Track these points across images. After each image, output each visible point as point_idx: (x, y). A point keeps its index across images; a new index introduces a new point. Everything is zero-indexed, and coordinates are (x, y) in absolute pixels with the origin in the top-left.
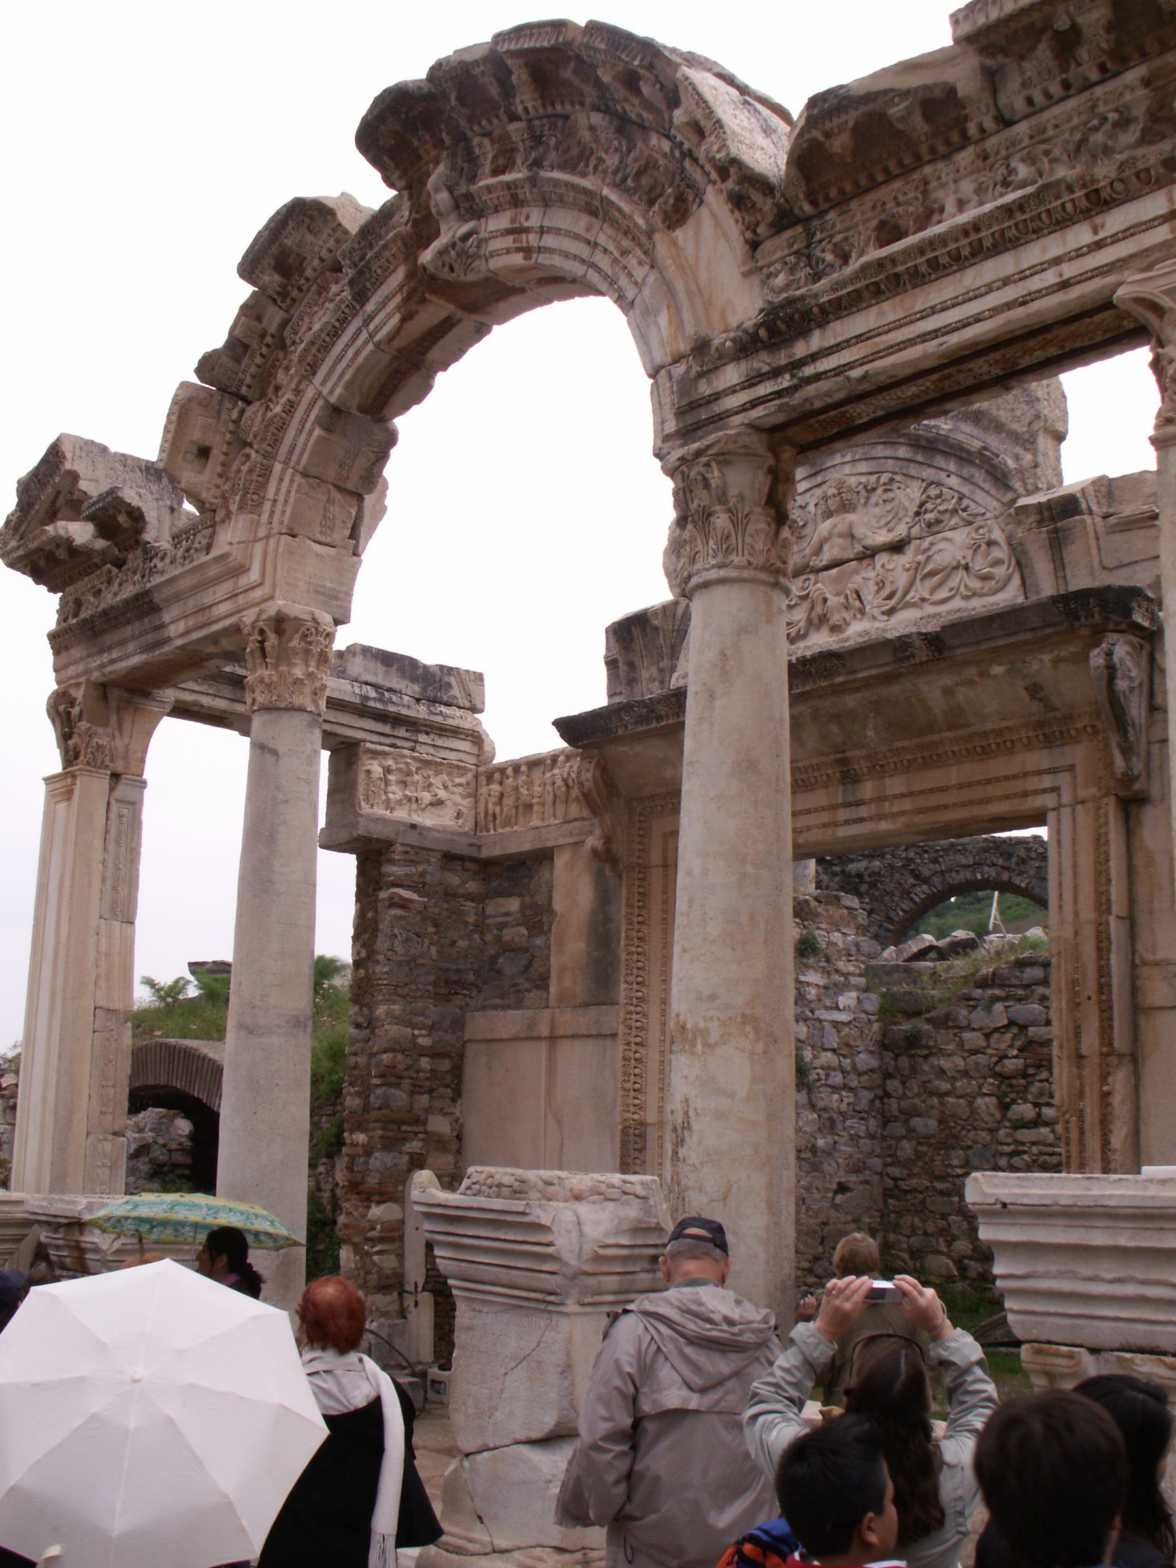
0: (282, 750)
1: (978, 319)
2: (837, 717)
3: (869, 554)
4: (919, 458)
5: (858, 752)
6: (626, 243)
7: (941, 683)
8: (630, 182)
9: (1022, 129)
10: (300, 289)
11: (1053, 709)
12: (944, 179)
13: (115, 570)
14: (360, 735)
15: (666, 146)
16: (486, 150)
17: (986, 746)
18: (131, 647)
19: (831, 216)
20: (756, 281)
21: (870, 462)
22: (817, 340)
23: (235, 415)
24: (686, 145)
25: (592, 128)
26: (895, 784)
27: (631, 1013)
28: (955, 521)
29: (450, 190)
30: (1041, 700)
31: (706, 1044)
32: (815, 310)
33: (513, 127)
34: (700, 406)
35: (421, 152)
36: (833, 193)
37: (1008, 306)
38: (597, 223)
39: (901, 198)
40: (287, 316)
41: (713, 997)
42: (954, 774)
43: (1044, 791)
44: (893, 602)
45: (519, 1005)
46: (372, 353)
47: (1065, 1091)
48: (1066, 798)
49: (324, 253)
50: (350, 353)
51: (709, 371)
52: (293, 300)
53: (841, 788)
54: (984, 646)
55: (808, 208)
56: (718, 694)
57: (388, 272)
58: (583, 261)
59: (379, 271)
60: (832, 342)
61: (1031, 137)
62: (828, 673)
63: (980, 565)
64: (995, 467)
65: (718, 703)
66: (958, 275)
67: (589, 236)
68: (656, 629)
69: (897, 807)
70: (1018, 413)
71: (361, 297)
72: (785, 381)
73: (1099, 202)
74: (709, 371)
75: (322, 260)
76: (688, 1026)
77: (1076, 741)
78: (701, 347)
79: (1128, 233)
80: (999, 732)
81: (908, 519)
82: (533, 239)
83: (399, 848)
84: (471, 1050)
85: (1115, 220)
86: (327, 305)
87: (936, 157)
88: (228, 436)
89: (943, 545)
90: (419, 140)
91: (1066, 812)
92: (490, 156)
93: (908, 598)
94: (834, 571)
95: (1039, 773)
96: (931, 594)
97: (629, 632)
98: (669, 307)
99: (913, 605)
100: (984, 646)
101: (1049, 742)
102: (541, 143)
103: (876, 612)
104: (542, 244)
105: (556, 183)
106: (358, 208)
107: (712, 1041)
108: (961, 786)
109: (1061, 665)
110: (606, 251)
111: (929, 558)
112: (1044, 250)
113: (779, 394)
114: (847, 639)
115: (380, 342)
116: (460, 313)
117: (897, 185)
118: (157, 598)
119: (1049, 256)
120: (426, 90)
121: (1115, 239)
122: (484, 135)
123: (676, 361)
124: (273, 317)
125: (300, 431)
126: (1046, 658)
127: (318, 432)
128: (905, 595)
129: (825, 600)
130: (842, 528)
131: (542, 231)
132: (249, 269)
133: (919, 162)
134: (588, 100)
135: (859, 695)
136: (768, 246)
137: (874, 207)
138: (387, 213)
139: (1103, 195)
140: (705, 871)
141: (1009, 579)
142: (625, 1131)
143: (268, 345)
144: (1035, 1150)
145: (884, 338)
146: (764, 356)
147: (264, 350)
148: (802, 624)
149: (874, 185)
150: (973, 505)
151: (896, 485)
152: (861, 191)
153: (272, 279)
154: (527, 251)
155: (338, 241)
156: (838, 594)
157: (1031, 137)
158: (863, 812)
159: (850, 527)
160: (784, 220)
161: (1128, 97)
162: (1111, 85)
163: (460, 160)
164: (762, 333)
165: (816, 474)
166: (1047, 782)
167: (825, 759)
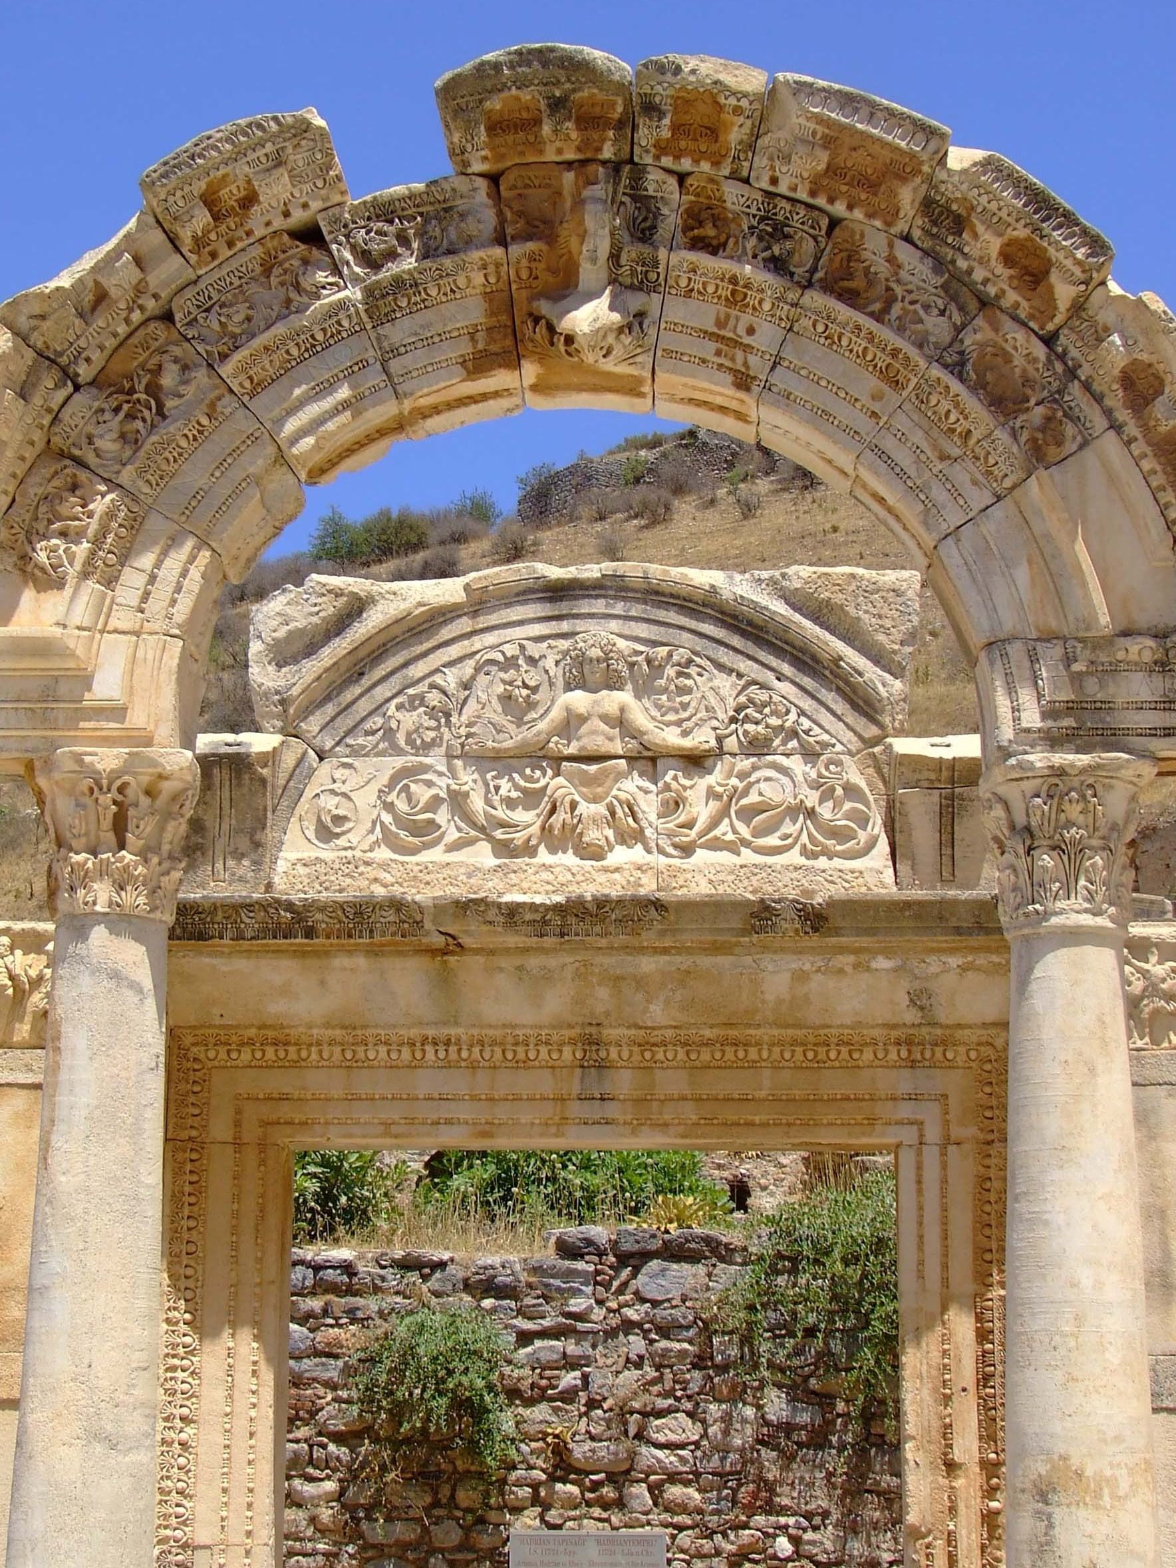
7: (794, 966)
10: (230, 244)
15: (1040, 351)
21: (654, 628)
25: (891, 259)
27: (173, 1369)
30: (922, 1008)
31: (1113, 1496)
38: (893, 398)
43: (900, 1123)
44: (693, 834)
48: (933, 1134)
52: (213, 255)
53: (578, 1071)
64: (854, 688)
65: (1102, 1080)
67: (876, 407)
77: (951, 1066)
81: (715, 723)
90: (556, 131)
91: (931, 1156)
93: (717, 832)
94: (593, 768)
95: (894, 1099)
98: (1030, 562)
101: (913, 1064)
102: (787, 237)
103: (664, 842)
104: (772, 380)
107: (1121, 1493)
109: (969, 973)
114: (617, 870)
123: (1048, 638)
124: (169, 270)
126: (954, 961)
129: (574, 805)
135: (667, 958)
143: (141, 308)
148: (535, 829)
150: (817, 730)
151: (693, 670)
154: (743, 382)
156: (595, 800)
158: (612, 1110)
159: (622, 710)
166: (905, 1111)
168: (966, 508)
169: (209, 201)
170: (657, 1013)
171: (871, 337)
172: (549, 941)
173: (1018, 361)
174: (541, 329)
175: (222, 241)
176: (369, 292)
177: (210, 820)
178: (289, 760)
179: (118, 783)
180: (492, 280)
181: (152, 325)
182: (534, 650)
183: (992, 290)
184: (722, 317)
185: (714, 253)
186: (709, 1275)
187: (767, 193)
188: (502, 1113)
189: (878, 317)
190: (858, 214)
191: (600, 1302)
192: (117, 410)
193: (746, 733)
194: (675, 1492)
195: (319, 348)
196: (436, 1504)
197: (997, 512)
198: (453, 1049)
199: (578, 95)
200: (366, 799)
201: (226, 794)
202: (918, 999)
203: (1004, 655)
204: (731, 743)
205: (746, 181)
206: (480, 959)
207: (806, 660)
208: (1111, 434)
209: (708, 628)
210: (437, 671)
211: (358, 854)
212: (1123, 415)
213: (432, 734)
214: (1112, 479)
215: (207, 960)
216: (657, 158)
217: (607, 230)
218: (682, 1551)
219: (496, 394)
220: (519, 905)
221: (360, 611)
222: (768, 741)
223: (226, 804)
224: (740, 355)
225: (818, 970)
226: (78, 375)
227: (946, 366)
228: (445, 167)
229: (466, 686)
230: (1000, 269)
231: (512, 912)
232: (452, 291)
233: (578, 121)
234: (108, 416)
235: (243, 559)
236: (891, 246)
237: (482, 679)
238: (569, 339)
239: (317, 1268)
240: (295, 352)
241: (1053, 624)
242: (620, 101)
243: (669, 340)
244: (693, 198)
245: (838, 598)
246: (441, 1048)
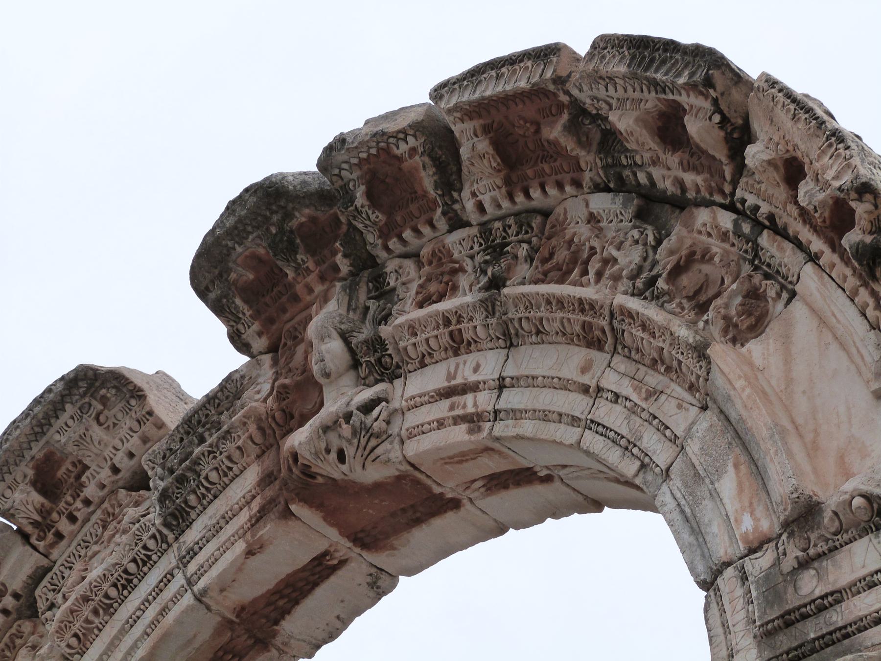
6: (654, 379)
8: (661, 284)
10: (72, 519)
15: (726, 220)
16: (405, 277)
24: (765, 208)
25: (593, 219)
29: (345, 337)
34: (805, 617)
35: (299, 288)
38: (600, 358)
40: (45, 562)
46: (189, 610)
49: (120, 460)
50: (151, 613)
51: (820, 556)
52: (59, 536)
57: (228, 475)
58: (575, 421)
59: (213, 476)
67: (586, 379)
71: (178, 519)
74: (820, 556)
75: (115, 470)
78: (804, 515)
82: (484, 400)
86: (117, 538)
90: (297, 269)
92: (414, 287)
98: (736, 466)
102: (502, 254)
104: (502, 405)
105: (529, 303)
106: (181, 396)
115: (205, 592)
116: (344, 546)
120: (315, 186)
122: (405, 256)
131: (501, 386)
134: (587, 177)
138: (230, 390)
155: (145, 440)
163: (362, 295)
173: (717, 247)
175: (64, 518)
180: (258, 439)
184: (452, 370)
195: (135, 581)
199: (294, 224)
208: (809, 268)
217: (335, 334)
224: (469, 398)
228: (238, 360)
232: (230, 469)
233: (312, 251)
240: (113, 593)
243: (413, 419)
244: (427, 268)
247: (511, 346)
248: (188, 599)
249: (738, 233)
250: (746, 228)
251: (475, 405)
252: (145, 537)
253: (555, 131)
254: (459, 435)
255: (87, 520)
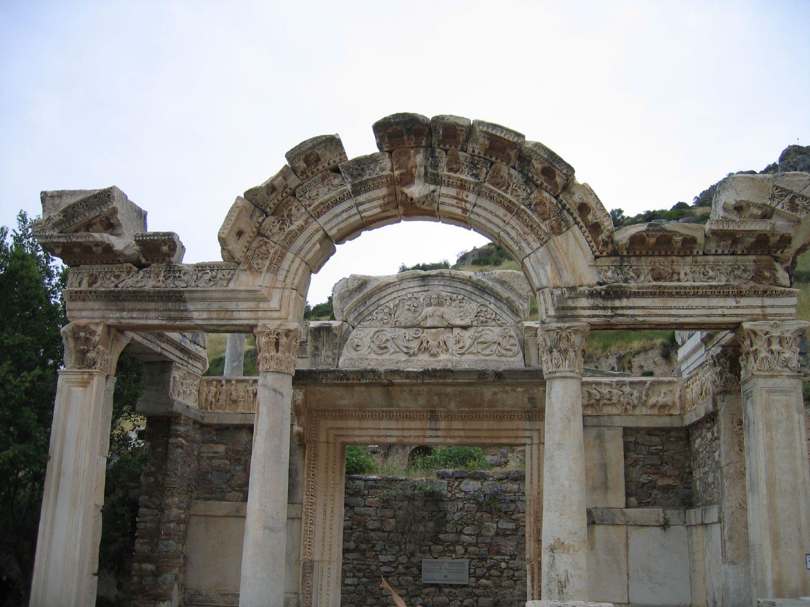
0: (285, 393)
1: (691, 316)
2: (439, 395)
3: (451, 327)
4: (477, 293)
5: (442, 409)
6: (527, 230)
7: (493, 390)
9: (711, 258)
11: (536, 407)
12: (680, 263)
13: (135, 269)
14: (174, 358)
15: (554, 201)
17: (501, 416)
18: (152, 314)
19: (633, 259)
20: (595, 269)
22: (625, 302)
23: (260, 220)
25: (509, 174)
26: (457, 424)
28: (493, 323)
29: (425, 168)
30: (532, 403)
31: (574, 551)
32: (628, 293)
33: (461, 154)
36: (638, 253)
37: (705, 315)
39: (662, 264)
41: (575, 533)
42: (485, 425)
43: (526, 437)
44: (464, 350)
45: (223, 499)
47: (532, 553)
48: (536, 441)
49: (331, 162)
50: (345, 215)
51: (574, 298)
53: (429, 422)
54: (519, 381)
55: (625, 253)
56: (572, 419)
59: (372, 186)
60: (632, 305)
61: (714, 262)
62: (445, 377)
63: (504, 343)
64: (513, 306)
65: (572, 423)
66: (685, 299)
67: (505, 218)
68: (336, 335)
69: (456, 434)
70: (523, 287)
71: (356, 192)
72: (609, 313)
73: (740, 294)
74: (574, 298)
75: (329, 164)
76: (566, 543)
79: (747, 307)
80: (509, 412)
82: (469, 206)
83: (183, 418)
84: (193, 520)
85: (744, 301)
87: (679, 255)
88: (255, 230)
89: (488, 332)
91: (535, 447)
94: (434, 330)
95: (524, 430)
96: (482, 351)
97: (319, 333)
98: (551, 265)
99: (474, 354)
100: (519, 381)
101: (530, 419)
108: (489, 430)
110: (513, 228)
111: (481, 335)
112: (718, 302)
113: (605, 316)
115: (365, 217)
117: (661, 259)
118: (186, 295)
119: (720, 305)
121: (743, 307)
122: (443, 149)
123: (556, 287)
124: (293, 181)
125: (306, 242)
127: (318, 246)
128: (468, 349)
129: (428, 342)
130: (438, 313)
131: (475, 205)
132: (291, 156)
133: (672, 254)
134: (512, 164)
136: (604, 259)
137: (651, 262)
139: (743, 293)
140: (570, 486)
141: (519, 352)
142: (305, 563)
143: (286, 193)
144: (355, 562)
145: (653, 310)
146: (600, 300)
147: (284, 195)
148: (416, 349)
149: (653, 255)
151: (464, 301)
152: (647, 255)
153: (303, 165)
154: (465, 210)
156: (434, 341)
157: (714, 262)
158: (439, 433)
160: (615, 253)
161: (748, 263)
162: (744, 258)
164: (603, 293)
165: (424, 286)
166: (527, 434)
167: (425, 409)
168: (532, 248)
169: (306, 161)
170: (452, 406)
171: (503, 197)
172: (419, 381)
173: (548, 204)
174: (404, 198)
176: (353, 186)
177: (320, 346)
178: (345, 328)
179: (276, 333)
180: (389, 181)
181: (289, 197)
182: (415, 295)
183: (539, 182)
185: (456, 172)
186: (482, 484)
187: (472, 155)
188: (407, 433)
189: (505, 191)
190: (499, 161)
191: (449, 492)
192: (278, 222)
193: (479, 320)
194: (471, 549)
196: (401, 550)
197: (542, 250)
198: (391, 414)
200: (367, 340)
201: (325, 339)
202: (531, 399)
203: (543, 293)
204: (475, 323)
205: (466, 152)
206: (399, 388)
207: (498, 298)
209: (469, 288)
210: (388, 302)
211: (363, 356)
212: (579, 219)
213: (386, 321)
214: (576, 239)
215: (318, 388)
216: (439, 145)
218: (473, 566)
219: (392, 217)
220: (410, 372)
221: (366, 284)
222: (486, 322)
223: (325, 342)
224: (463, 203)
225: (500, 392)
226: (267, 212)
227: (525, 206)
228: (377, 150)
229: (396, 306)
230: (541, 176)
231: (408, 375)
233: (415, 135)
234: (276, 223)
235: (317, 266)
236: (509, 170)
237: (401, 305)
238: (412, 199)
239: (366, 481)
240: (331, 204)
241: (558, 283)
242: (427, 129)
243: (442, 199)
245: (508, 280)
246: (388, 414)
247: (479, 195)
248: (358, 217)
249: (556, 205)
250: (560, 206)
251: (465, 206)
252: (345, 193)
253: (513, 153)
254: (459, 211)
255: (316, 175)
